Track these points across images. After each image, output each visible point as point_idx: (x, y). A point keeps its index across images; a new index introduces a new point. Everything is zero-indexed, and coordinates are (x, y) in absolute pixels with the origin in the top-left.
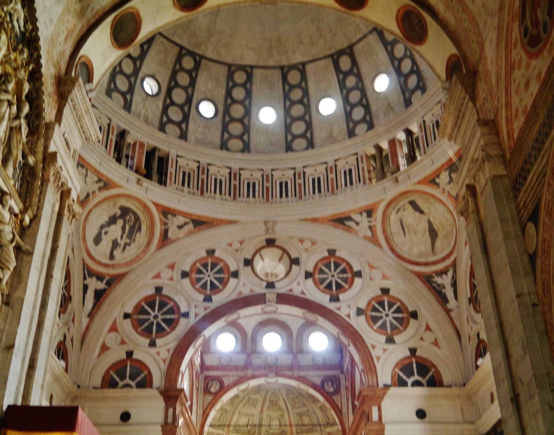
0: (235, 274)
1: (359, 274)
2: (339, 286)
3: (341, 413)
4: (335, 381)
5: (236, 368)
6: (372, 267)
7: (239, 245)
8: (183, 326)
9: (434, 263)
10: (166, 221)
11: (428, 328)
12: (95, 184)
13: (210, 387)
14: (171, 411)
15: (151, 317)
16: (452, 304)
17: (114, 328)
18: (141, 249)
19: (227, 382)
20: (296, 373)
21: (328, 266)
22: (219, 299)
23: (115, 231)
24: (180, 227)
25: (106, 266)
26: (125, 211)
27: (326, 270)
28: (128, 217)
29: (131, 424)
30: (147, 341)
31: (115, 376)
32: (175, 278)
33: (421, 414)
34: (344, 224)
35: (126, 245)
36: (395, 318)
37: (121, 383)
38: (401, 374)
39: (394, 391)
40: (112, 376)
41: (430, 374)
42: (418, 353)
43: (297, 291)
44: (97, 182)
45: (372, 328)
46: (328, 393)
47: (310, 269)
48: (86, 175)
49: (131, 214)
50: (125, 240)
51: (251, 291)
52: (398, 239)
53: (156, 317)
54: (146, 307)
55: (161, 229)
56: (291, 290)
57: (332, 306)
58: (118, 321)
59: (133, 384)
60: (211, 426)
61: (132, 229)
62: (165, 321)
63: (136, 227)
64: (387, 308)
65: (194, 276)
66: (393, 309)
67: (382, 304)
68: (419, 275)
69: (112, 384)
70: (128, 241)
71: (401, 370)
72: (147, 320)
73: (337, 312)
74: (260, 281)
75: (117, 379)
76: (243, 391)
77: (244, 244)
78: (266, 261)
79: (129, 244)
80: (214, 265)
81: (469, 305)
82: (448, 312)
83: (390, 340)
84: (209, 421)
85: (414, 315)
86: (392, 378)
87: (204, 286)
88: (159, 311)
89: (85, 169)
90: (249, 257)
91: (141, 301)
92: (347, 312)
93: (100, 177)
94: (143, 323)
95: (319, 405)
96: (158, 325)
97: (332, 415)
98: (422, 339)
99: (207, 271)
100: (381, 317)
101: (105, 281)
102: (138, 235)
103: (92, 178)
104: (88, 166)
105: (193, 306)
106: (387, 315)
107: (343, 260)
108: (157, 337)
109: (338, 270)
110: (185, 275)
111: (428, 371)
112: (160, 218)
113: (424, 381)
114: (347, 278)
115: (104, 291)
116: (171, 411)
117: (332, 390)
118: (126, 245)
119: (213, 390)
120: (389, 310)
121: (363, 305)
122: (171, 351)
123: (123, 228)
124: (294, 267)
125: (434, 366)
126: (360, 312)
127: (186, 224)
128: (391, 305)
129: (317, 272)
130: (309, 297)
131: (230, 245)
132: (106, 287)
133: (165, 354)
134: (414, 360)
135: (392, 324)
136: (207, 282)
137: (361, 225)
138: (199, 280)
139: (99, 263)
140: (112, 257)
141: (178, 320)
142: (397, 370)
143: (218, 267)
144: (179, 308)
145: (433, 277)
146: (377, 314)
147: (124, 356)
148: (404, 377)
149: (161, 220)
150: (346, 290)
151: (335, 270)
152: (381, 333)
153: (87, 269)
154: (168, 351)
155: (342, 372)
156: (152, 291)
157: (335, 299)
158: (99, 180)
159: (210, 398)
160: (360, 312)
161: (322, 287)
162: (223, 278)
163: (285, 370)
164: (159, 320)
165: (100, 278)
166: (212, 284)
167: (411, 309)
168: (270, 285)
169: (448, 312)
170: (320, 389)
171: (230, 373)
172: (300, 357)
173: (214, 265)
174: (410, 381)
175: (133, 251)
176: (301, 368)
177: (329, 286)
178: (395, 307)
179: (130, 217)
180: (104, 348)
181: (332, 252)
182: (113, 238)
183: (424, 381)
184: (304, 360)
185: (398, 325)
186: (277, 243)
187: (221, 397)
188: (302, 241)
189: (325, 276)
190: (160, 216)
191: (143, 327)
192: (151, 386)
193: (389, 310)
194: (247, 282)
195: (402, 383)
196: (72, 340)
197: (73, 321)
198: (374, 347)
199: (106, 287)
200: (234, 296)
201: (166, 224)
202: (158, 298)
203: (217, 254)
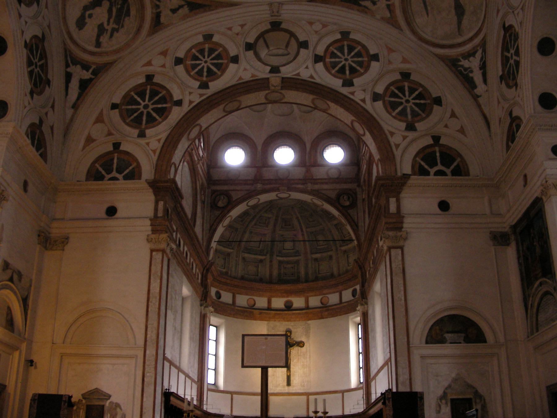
0: (235, 60)
1: (375, 57)
2: (353, 71)
3: (357, 226)
4: (352, 195)
5: (245, 182)
6: (390, 50)
7: (240, 28)
8: (176, 114)
9: (460, 45)
11: (453, 115)
13: (219, 201)
14: (161, 204)
15: (141, 107)
16: (481, 88)
17: (99, 120)
18: (131, 36)
19: (235, 196)
20: (310, 187)
21: (341, 49)
22: (216, 86)
24: (174, 11)
25: (92, 54)
27: (339, 54)
29: (117, 218)
30: (136, 132)
31: (101, 169)
32: (167, 65)
33: (444, 206)
34: (360, 5)
36: (416, 104)
37: (108, 177)
38: (422, 163)
39: (415, 180)
40: (98, 169)
41: (455, 164)
42: (442, 142)
43: (305, 74)
45: (390, 114)
46: (344, 207)
47: (320, 50)
50: (112, 25)
51: (253, 76)
52: (420, 21)
53: (146, 107)
54: (136, 97)
55: (152, 13)
56: (298, 74)
57: (345, 91)
58: (105, 112)
59: (120, 176)
60: (219, 242)
61: (119, 11)
62: (155, 110)
64: (407, 93)
65: (189, 62)
66: (414, 95)
67: (401, 89)
68: (442, 58)
69: (99, 177)
70: (116, 27)
71: (422, 159)
72: (136, 110)
73: (352, 97)
74: (263, 66)
75: (103, 172)
76: (254, 207)
77: (246, 27)
78: (271, 49)
79: (117, 30)
80: (211, 51)
81: (500, 83)
82: (476, 97)
83: (411, 127)
84: (217, 236)
85: (438, 101)
86: (413, 167)
87: (200, 73)
88: (149, 101)
90: (251, 40)
91: (130, 90)
92: (362, 97)
94: (133, 114)
95: (335, 222)
96: (149, 114)
97: (349, 233)
98: (446, 126)
99: (204, 57)
100: (401, 103)
101: (91, 71)
102: (126, 19)
105: (187, 93)
106: (408, 101)
107: (359, 43)
108: (147, 128)
109: (353, 54)
110: (178, 61)
111: (453, 160)
113: (448, 171)
114: (362, 62)
115: (91, 80)
116: (161, 204)
117: (347, 203)
118: (114, 30)
119: (220, 204)
120: (409, 97)
121: (380, 89)
122: (162, 141)
123: (110, 11)
124: (302, 51)
125: (460, 155)
126: (376, 97)
127: (181, 7)
128: (412, 91)
129: (328, 56)
130: (318, 81)
131: (230, 29)
132: (93, 77)
133: (156, 145)
134: (437, 149)
135: (413, 111)
136: (203, 67)
137: (379, 4)
138: (194, 67)
139: (85, 50)
140: (98, 44)
141: (171, 108)
142: (418, 159)
143: (216, 53)
144: (171, 96)
145: (460, 61)
146: (397, 100)
147: (111, 149)
148: (426, 167)
150: (362, 74)
151: (349, 53)
152: (400, 120)
153: (70, 56)
154: (159, 140)
155: (359, 186)
156: (142, 80)
157: (348, 83)
159: (217, 213)
160: (376, 97)
161: (333, 72)
162: (222, 64)
163: (298, 184)
164: (149, 109)
166: (209, 70)
167: (434, 96)
168: (275, 70)
169: (476, 97)
170: (335, 202)
171: (239, 188)
172: (314, 170)
173: (211, 51)
174: (432, 171)
175: (121, 38)
176: (315, 181)
177: (342, 70)
178: (417, 93)
180: (90, 140)
181: (345, 34)
182: (99, 23)
183: (448, 171)
184: (319, 173)
185: (420, 112)
186: (283, 26)
187: (229, 211)
188: (311, 23)
189: (337, 60)
191: (132, 117)
192: (140, 178)
193: (409, 97)
194: (248, 67)
195: (423, 172)
196: (52, 128)
197: (53, 107)
198: (392, 134)
199: (93, 77)
200: (234, 82)
201: (158, 7)
202: (149, 87)
203: (215, 39)
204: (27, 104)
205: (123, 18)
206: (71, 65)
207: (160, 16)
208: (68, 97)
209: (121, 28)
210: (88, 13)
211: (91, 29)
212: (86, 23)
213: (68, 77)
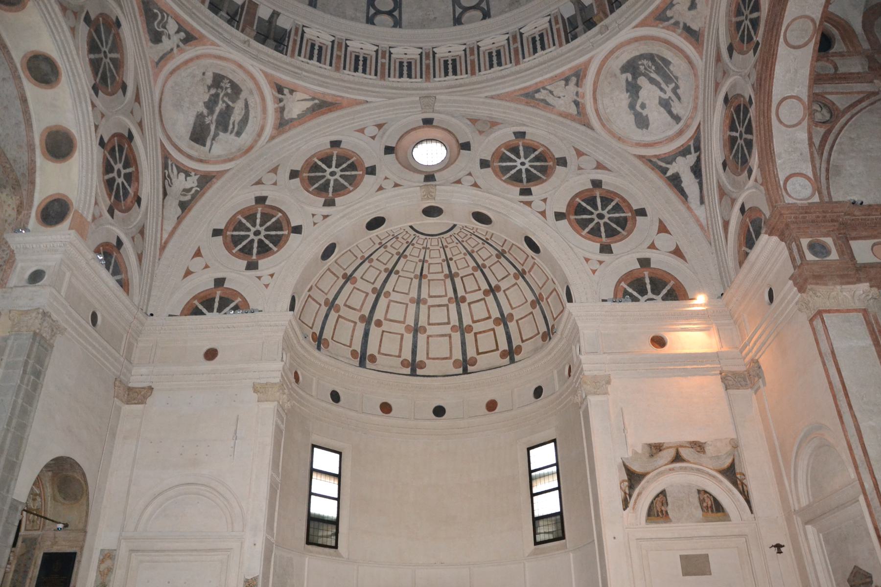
10: (672, 21)
12: (567, 87)
23: (649, 93)
25: (681, 133)
26: (631, 67)
28: (642, 68)
35: (675, 91)
44: (567, 84)
48: (551, 92)
49: (640, 63)
50: (669, 89)
61: (659, 70)
63: (661, 65)
70: (672, 85)
79: (677, 87)
89: (542, 90)
93: (563, 77)
103: (559, 88)
104: (540, 86)
112: (663, 28)
115: (699, 159)
118: (675, 91)
123: (652, 81)
132: (698, 153)
139: (671, 139)
140: (677, 118)
149: (667, 28)
153: (659, 160)
158: (567, 80)
165: (684, 152)
179: (643, 65)
182: (657, 101)
190: (661, 26)
199: (698, 153)
201: (677, 24)
204: (596, 266)
205: (668, 72)
206: (668, 166)
207: (689, 27)
208: (688, 199)
209: (677, 81)
210: (638, 108)
211: (656, 115)
212: (647, 116)
213: (675, 181)
